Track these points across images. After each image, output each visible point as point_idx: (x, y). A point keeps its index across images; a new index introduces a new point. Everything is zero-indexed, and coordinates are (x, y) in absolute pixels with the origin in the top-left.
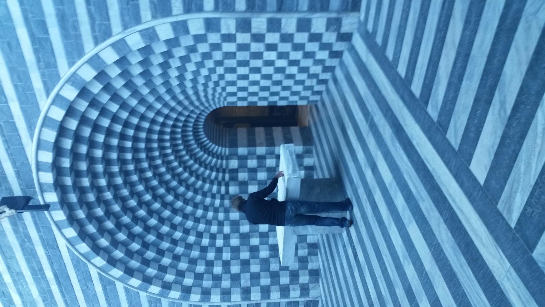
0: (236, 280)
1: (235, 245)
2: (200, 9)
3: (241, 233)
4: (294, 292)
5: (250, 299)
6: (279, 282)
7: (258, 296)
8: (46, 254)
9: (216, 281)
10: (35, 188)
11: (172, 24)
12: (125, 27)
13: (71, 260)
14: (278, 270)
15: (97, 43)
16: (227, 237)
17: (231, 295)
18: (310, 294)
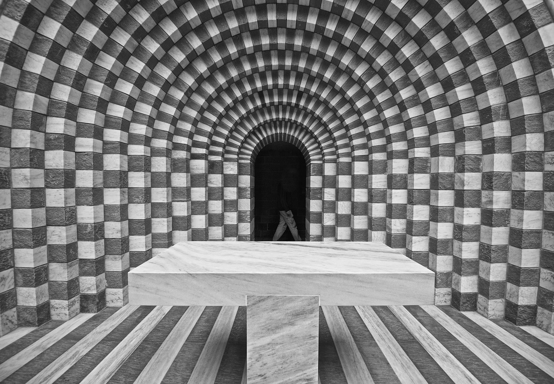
0: (31, 160)
1: (105, 163)
3: (127, 174)
6: (22, 247)
9: (30, 119)
14: (50, 243)
16: (122, 148)
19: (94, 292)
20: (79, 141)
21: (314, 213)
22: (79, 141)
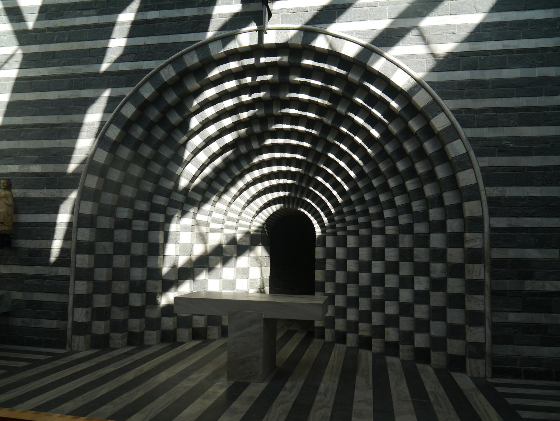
2: (492, 214)
4: (84, 313)
5: (77, 252)
7: (82, 264)
8: (187, 17)
10: (283, 23)
11: (477, 185)
12: (472, 141)
13: (174, 43)
15: (453, 111)
17: (89, 229)
18: (77, 336)
19: (138, 331)
20: (135, 222)
21: (318, 282)
22: (135, 222)
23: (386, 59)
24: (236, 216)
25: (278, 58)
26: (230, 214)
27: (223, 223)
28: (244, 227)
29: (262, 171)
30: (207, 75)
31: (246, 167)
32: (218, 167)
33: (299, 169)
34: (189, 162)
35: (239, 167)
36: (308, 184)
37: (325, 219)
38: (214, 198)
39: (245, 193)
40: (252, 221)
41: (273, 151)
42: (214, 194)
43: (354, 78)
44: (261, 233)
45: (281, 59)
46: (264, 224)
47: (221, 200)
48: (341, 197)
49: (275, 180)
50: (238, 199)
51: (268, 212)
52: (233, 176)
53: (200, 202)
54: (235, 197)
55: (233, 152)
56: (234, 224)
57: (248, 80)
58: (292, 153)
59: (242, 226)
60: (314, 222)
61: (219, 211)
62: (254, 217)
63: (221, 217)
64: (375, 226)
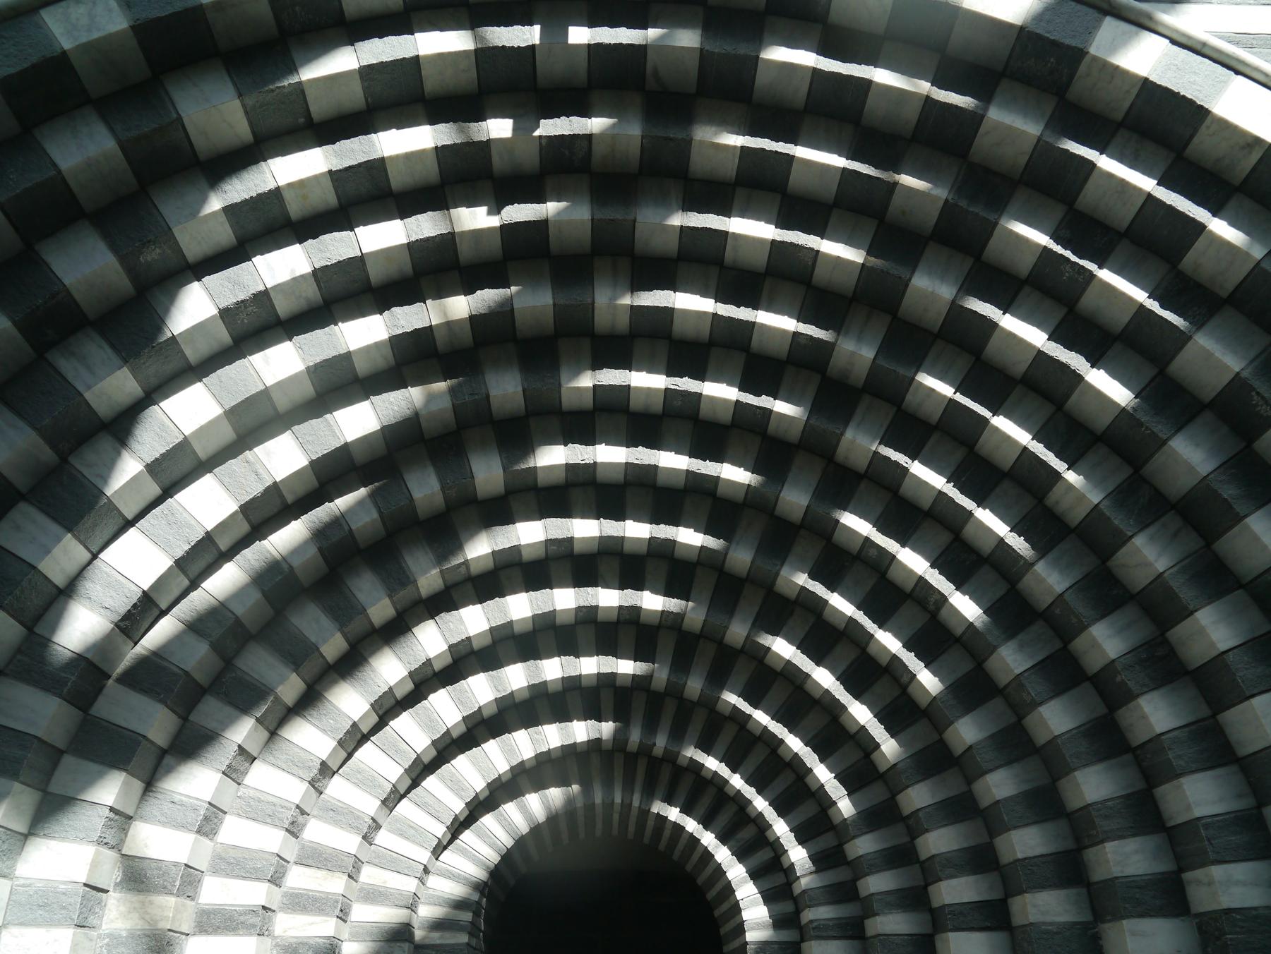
23: (1168, 41)
24: (349, 842)
25: (653, 33)
26: (317, 832)
27: (276, 880)
28: (382, 904)
29: (504, 611)
30: (293, 69)
31: (429, 580)
32: (285, 566)
33: (684, 602)
34: (129, 524)
35: (397, 579)
36: (718, 679)
37: (798, 855)
38: (243, 731)
39: (404, 723)
40: (426, 871)
41: (564, 511)
42: (245, 708)
43: (1014, 125)
44: (471, 934)
45: (662, 37)
46: (480, 887)
47: (279, 748)
48: (893, 731)
49: (556, 660)
50: (367, 754)
51: (506, 824)
52: (357, 626)
53: (163, 753)
54: (355, 738)
55: (372, 495)
56: (335, 884)
57: (499, 128)
58: (655, 520)
59: (373, 895)
60: (736, 872)
61: (260, 811)
62: (439, 849)
63: (270, 839)
64: (1130, 871)
